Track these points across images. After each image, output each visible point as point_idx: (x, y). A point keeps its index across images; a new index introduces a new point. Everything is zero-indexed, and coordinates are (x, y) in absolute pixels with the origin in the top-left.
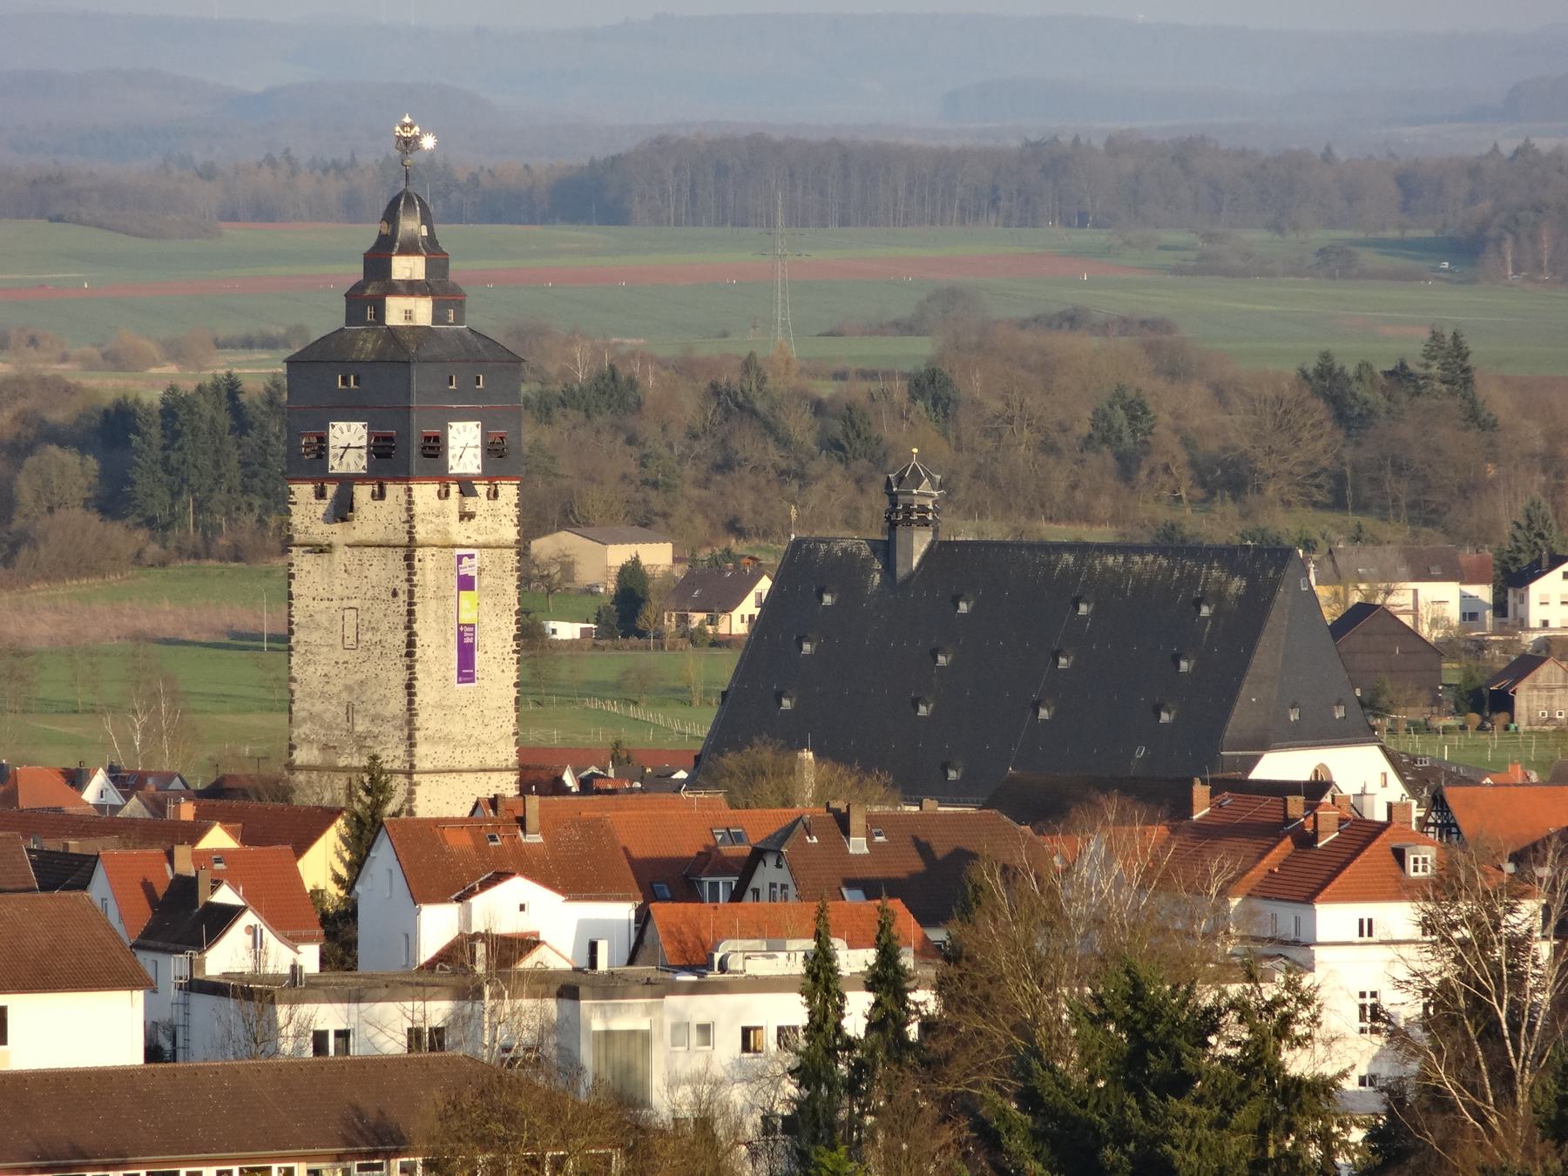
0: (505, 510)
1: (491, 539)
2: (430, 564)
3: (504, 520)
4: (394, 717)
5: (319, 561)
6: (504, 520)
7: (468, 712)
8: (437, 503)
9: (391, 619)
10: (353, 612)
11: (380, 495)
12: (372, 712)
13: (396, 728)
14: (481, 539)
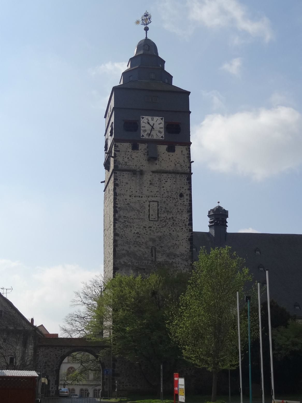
4: (182, 255)
5: (133, 178)
12: (168, 252)
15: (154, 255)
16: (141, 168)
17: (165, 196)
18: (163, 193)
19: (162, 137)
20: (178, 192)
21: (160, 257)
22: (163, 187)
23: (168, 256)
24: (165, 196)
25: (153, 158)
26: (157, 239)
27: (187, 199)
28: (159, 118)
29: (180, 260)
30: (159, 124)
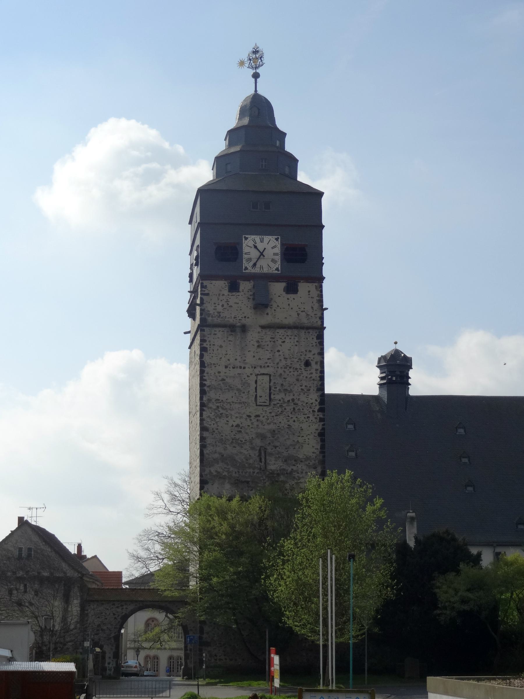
4: (308, 458)
9: (304, 383)
10: (267, 378)
11: (292, 289)
12: (285, 454)
13: (309, 466)
15: (263, 460)
16: (244, 321)
17: (281, 365)
18: (277, 360)
20: (302, 359)
21: (273, 462)
22: (279, 351)
23: (286, 461)
24: (281, 365)
25: (261, 305)
26: (269, 435)
27: (317, 370)
29: (304, 467)
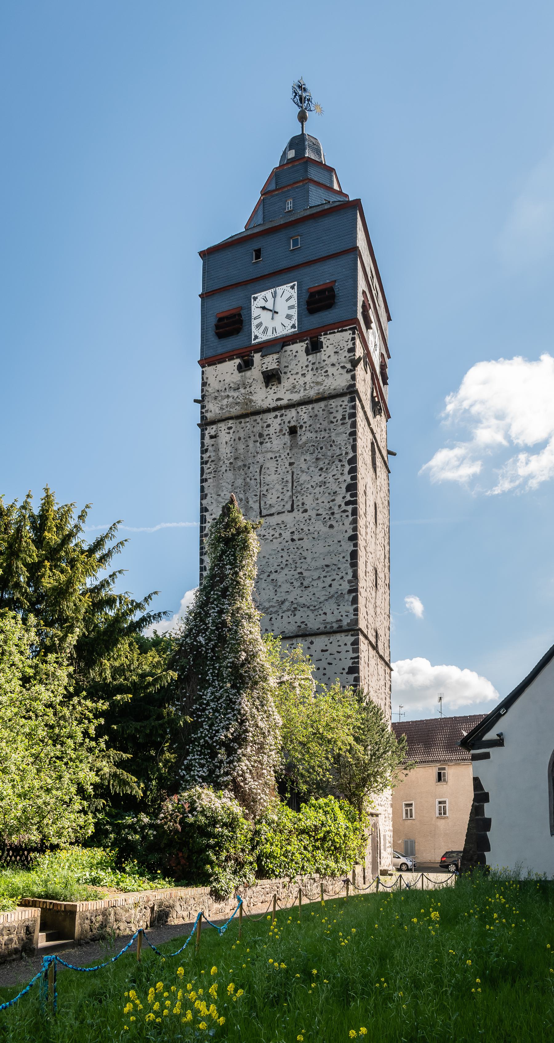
0: (334, 359)
1: (312, 393)
2: (224, 437)
3: (331, 370)
6: (331, 370)
7: (280, 578)
8: (237, 377)
14: (296, 397)
19: (293, 327)
28: (287, 287)
30: (287, 300)
